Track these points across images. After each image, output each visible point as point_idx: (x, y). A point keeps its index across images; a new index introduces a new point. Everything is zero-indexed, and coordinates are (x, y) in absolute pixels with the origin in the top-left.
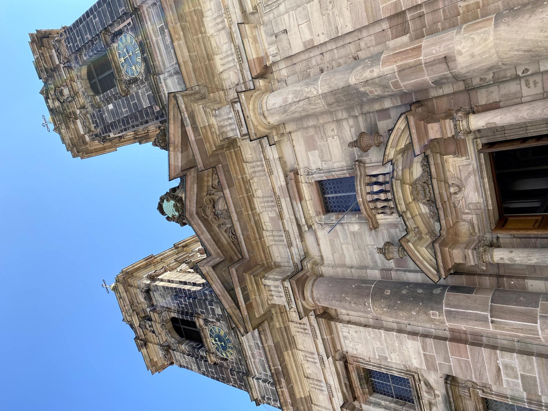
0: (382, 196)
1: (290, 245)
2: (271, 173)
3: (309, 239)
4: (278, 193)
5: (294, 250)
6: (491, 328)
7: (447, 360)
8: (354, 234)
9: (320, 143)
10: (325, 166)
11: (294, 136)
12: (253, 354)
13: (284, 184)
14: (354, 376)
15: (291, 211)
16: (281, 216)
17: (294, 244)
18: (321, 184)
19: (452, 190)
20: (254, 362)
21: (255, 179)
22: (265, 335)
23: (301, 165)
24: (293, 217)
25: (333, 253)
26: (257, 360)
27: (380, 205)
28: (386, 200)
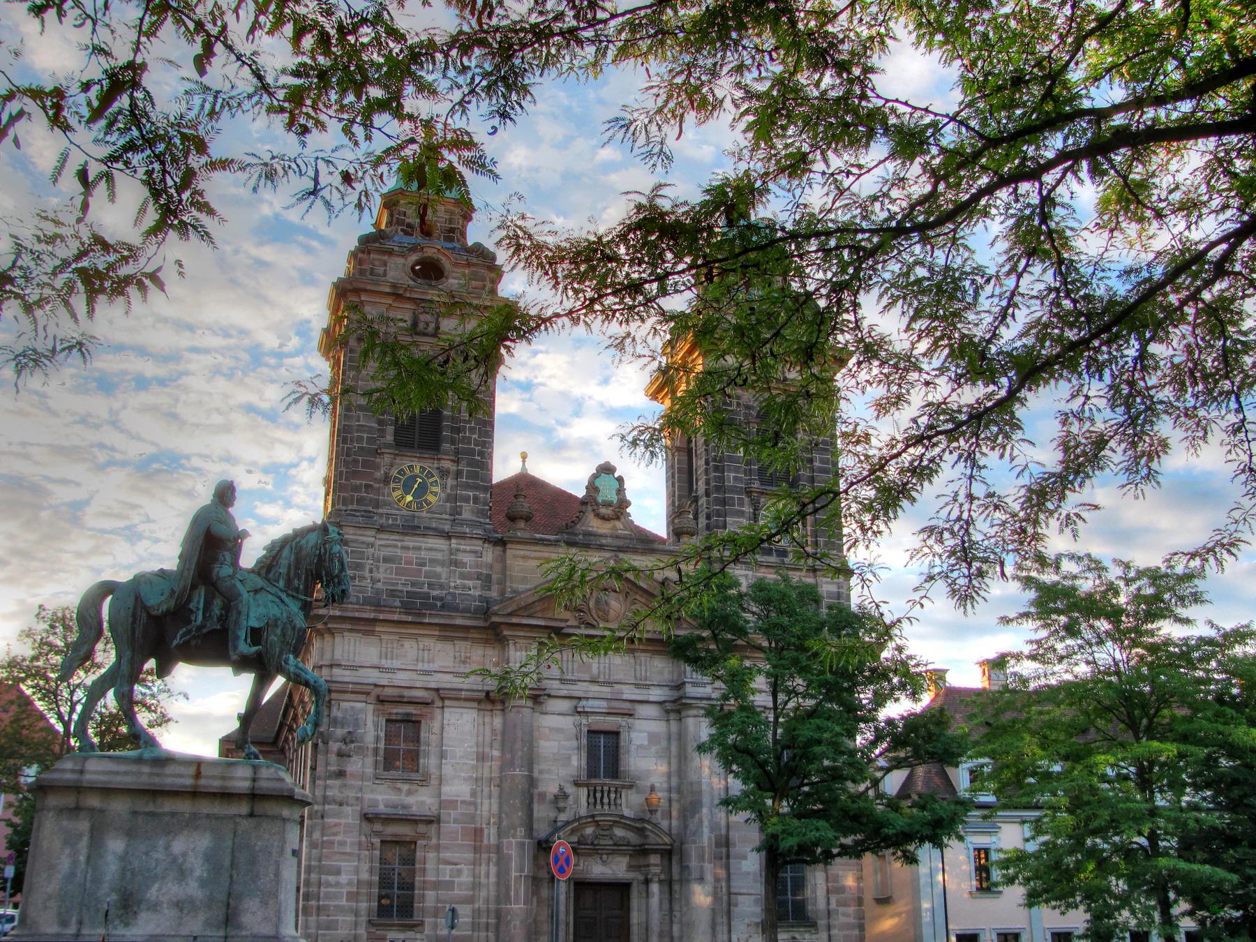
0: (599, 795)
1: (563, 681)
2: (637, 686)
3: (565, 705)
4: (617, 687)
5: (556, 684)
6: (514, 874)
7: (455, 821)
8: (569, 758)
9: (653, 749)
10: (633, 748)
11: (663, 724)
12: (407, 548)
13: (625, 697)
14: (411, 709)
15: (596, 695)
16: (593, 681)
17: (562, 686)
18: (617, 734)
19: (605, 857)
20: (396, 546)
21: (632, 661)
22: (469, 618)
23: (637, 722)
24: (591, 695)
25: (551, 729)
26: (399, 552)
27: (599, 795)
28: (602, 804)
